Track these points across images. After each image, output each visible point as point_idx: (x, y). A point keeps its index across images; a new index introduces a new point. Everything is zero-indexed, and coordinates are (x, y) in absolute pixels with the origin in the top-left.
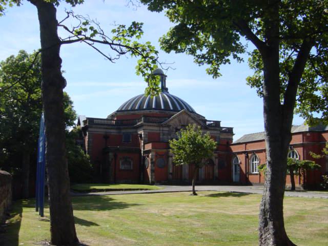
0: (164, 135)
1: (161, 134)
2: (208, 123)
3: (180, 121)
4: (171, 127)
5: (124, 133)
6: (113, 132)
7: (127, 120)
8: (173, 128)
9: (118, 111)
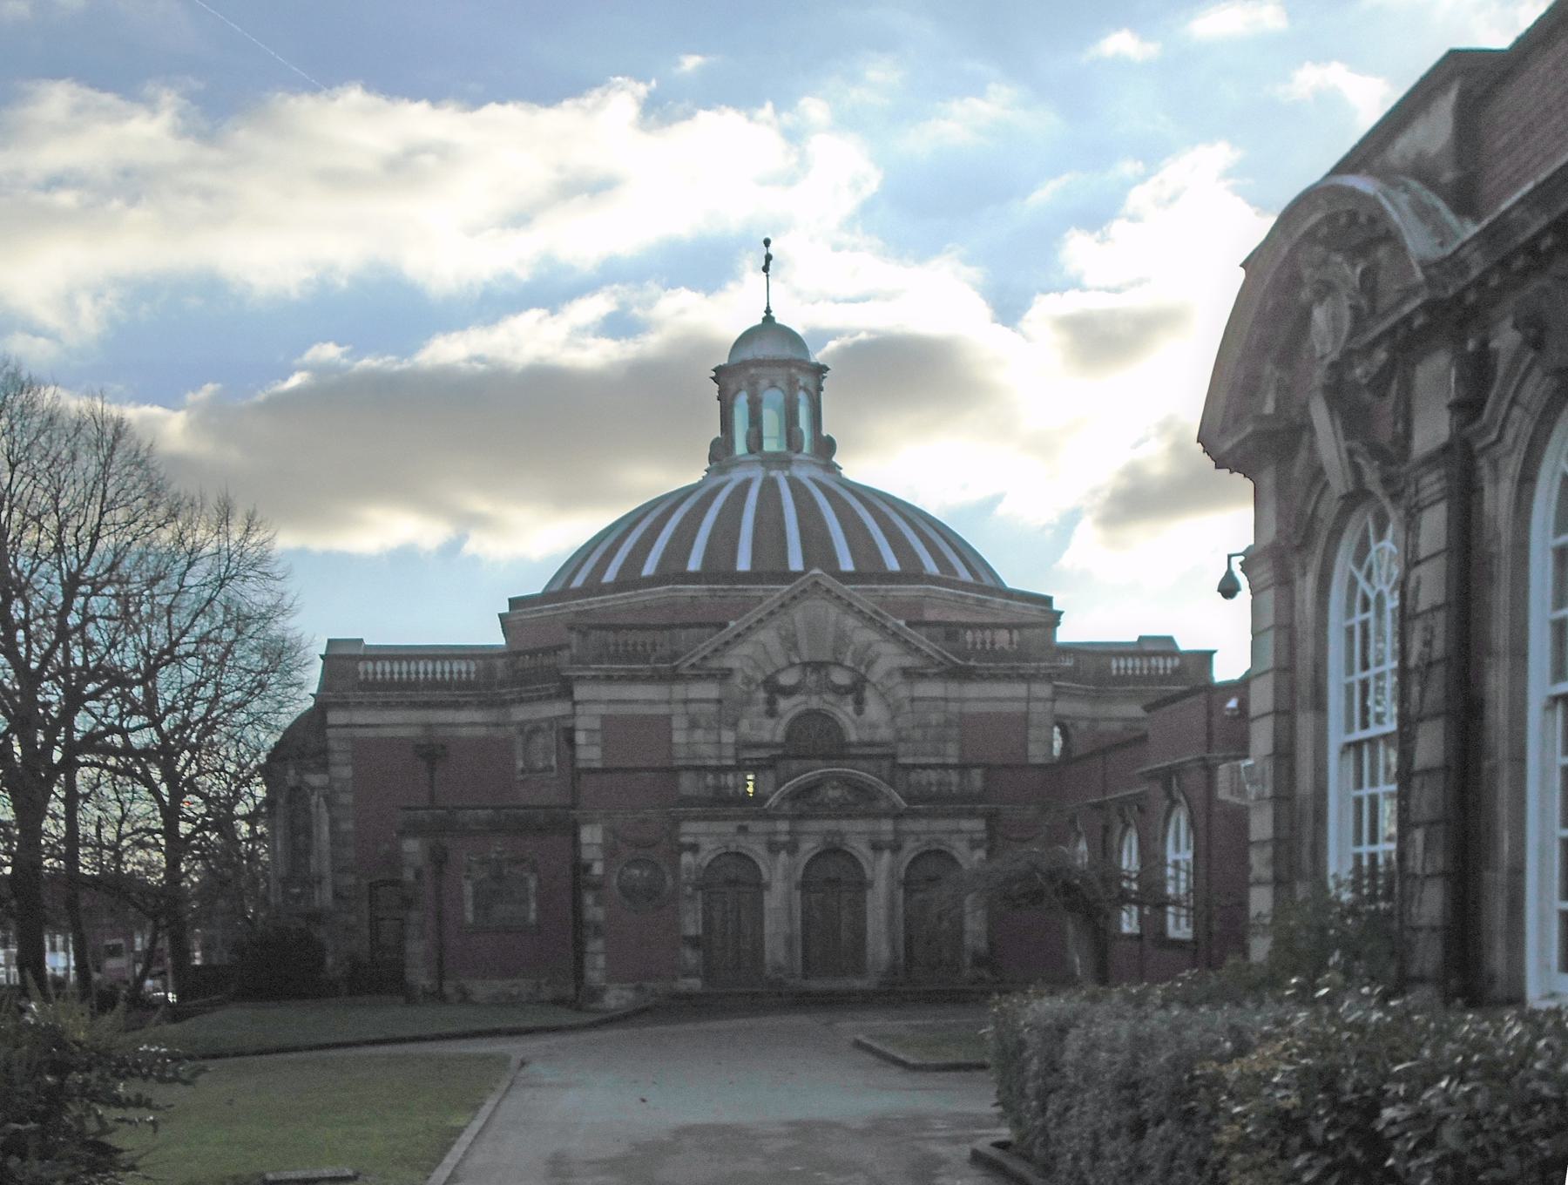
0: (693, 725)
1: (679, 723)
3: (790, 641)
4: (738, 679)
5: (521, 724)
6: (468, 721)
8: (749, 681)
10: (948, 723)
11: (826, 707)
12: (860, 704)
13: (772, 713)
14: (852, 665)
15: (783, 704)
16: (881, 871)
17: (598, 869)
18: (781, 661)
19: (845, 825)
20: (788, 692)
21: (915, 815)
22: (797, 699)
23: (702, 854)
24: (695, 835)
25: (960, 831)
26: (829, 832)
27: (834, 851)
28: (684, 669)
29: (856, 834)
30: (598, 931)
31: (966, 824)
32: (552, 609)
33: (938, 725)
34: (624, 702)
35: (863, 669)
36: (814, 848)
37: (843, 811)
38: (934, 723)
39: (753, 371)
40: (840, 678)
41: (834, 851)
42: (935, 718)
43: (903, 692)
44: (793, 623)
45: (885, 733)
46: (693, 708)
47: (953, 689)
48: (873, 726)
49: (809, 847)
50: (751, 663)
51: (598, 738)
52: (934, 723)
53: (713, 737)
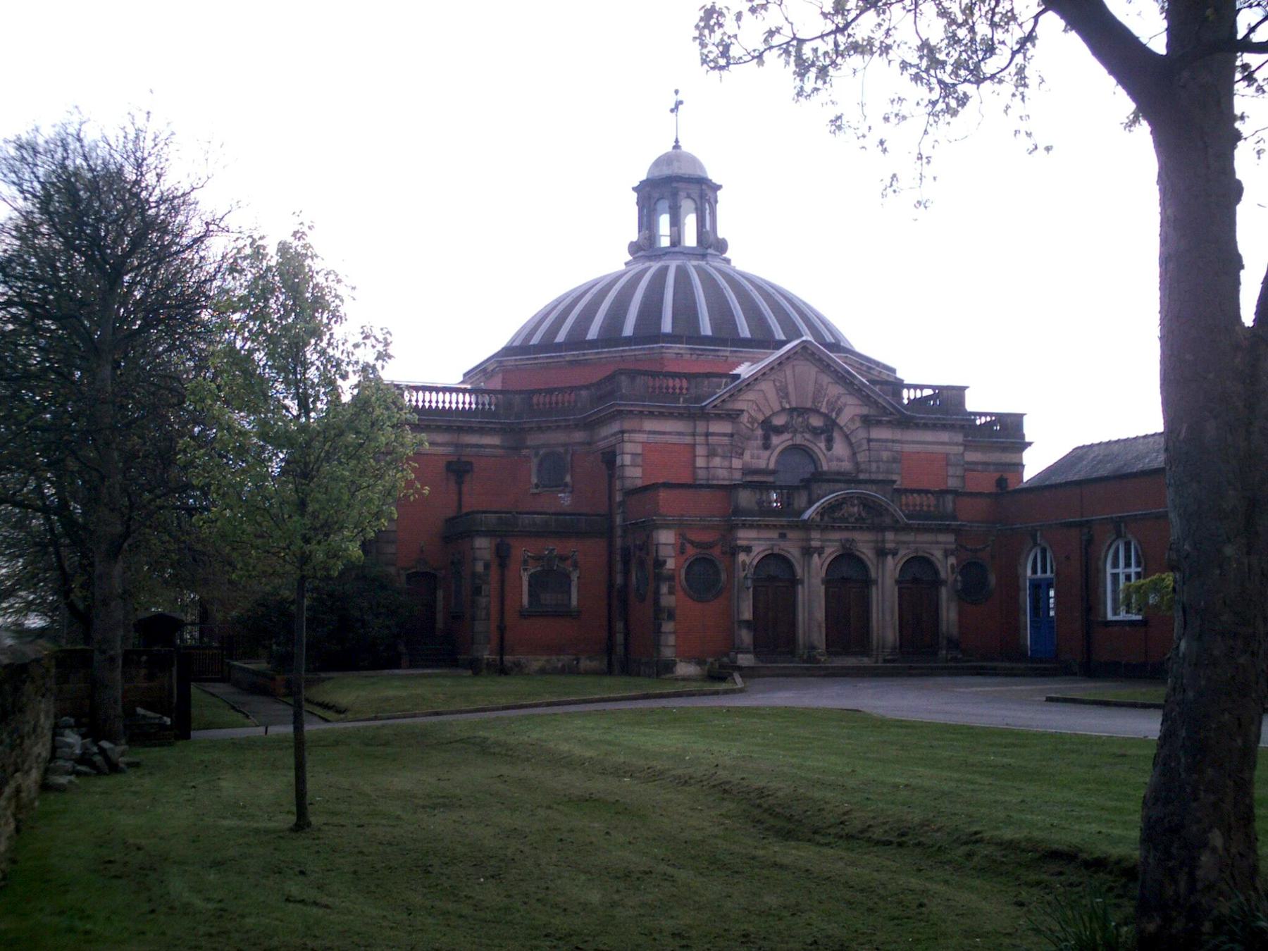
0: (711, 454)
1: (700, 450)
2: (907, 395)
3: (783, 392)
4: (744, 418)
7: (550, 391)
8: (753, 420)
9: (508, 351)
10: (894, 460)
11: (806, 443)
12: (829, 441)
13: (767, 446)
14: (827, 412)
15: (775, 440)
16: (887, 574)
17: (670, 564)
18: (777, 407)
19: (857, 536)
20: (779, 431)
21: (907, 528)
22: (786, 436)
23: (753, 554)
24: (748, 539)
25: (937, 543)
26: (847, 540)
27: (848, 556)
28: (709, 409)
29: (864, 545)
30: (671, 616)
31: (942, 538)
32: (547, 357)
33: (888, 462)
34: (664, 433)
35: (834, 415)
36: (833, 552)
37: (859, 525)
38: (885, 459)
39: (674, 185)
40: (816, 422)
41: (848, 556)
42: (885, 455)
43: (862, 434)
44: (786, 377)
45: (847, 466)
46: (712, 439)
47: (898, 434)
48: (839, 460)
49: (831, 551)
50: (754, 406)
51: (639, 460)
52: (885, 459)
53: (726, 464)
